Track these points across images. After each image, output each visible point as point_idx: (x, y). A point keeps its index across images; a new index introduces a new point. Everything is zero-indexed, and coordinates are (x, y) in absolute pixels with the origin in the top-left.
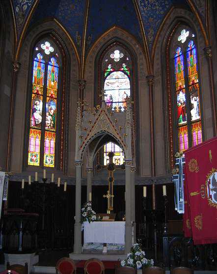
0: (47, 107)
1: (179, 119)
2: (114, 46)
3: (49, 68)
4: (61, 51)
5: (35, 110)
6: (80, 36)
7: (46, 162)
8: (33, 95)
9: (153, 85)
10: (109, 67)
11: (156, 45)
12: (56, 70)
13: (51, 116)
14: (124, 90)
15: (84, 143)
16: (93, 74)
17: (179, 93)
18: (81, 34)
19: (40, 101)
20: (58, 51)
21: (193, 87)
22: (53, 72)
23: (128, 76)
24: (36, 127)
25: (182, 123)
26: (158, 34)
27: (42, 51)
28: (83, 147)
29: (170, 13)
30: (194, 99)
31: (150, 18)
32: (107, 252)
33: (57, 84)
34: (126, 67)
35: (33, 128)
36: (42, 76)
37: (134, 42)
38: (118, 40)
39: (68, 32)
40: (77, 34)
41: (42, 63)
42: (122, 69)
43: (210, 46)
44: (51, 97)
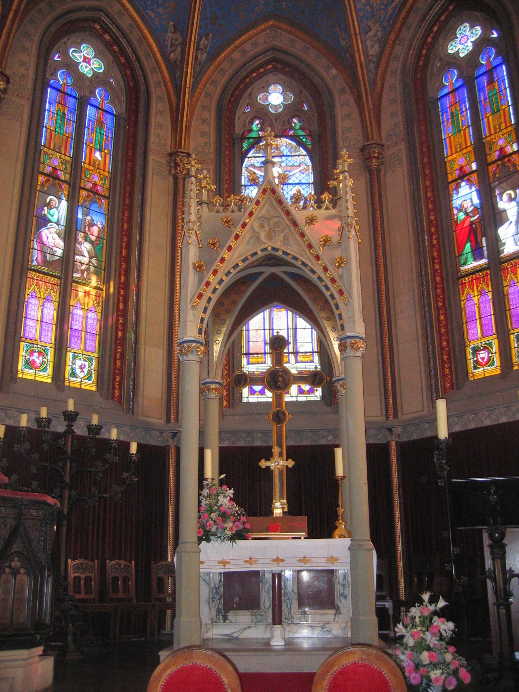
0: (80, 216)
1: (461, 254)
2: (265, 74)
3: (90, 112)
4: (124, 75)
5: (45, 221)
6: (178, 36)
7: (73, 374)
8: (41, 179)
9: (383, 168)
10: (256, 125)
12: (109, 121)
13: (91, 242)
14: (297, 187)
15: (208, 284)
16: (212, 139)
17: (458, 186)
19: (60, 199)
21: (503, 164)
23: (305, 148)
24: (45, 269)
25: (473, 264)
28: (205, 299)
30: (505, 197)
32: (286, 644)
34: (301, 128)
36: (70, 130)
37: (324, 62)
38: (279, 55)
40: (171, 28)
41: (70, 95)
42: (291, 132)
44: (94, 191)
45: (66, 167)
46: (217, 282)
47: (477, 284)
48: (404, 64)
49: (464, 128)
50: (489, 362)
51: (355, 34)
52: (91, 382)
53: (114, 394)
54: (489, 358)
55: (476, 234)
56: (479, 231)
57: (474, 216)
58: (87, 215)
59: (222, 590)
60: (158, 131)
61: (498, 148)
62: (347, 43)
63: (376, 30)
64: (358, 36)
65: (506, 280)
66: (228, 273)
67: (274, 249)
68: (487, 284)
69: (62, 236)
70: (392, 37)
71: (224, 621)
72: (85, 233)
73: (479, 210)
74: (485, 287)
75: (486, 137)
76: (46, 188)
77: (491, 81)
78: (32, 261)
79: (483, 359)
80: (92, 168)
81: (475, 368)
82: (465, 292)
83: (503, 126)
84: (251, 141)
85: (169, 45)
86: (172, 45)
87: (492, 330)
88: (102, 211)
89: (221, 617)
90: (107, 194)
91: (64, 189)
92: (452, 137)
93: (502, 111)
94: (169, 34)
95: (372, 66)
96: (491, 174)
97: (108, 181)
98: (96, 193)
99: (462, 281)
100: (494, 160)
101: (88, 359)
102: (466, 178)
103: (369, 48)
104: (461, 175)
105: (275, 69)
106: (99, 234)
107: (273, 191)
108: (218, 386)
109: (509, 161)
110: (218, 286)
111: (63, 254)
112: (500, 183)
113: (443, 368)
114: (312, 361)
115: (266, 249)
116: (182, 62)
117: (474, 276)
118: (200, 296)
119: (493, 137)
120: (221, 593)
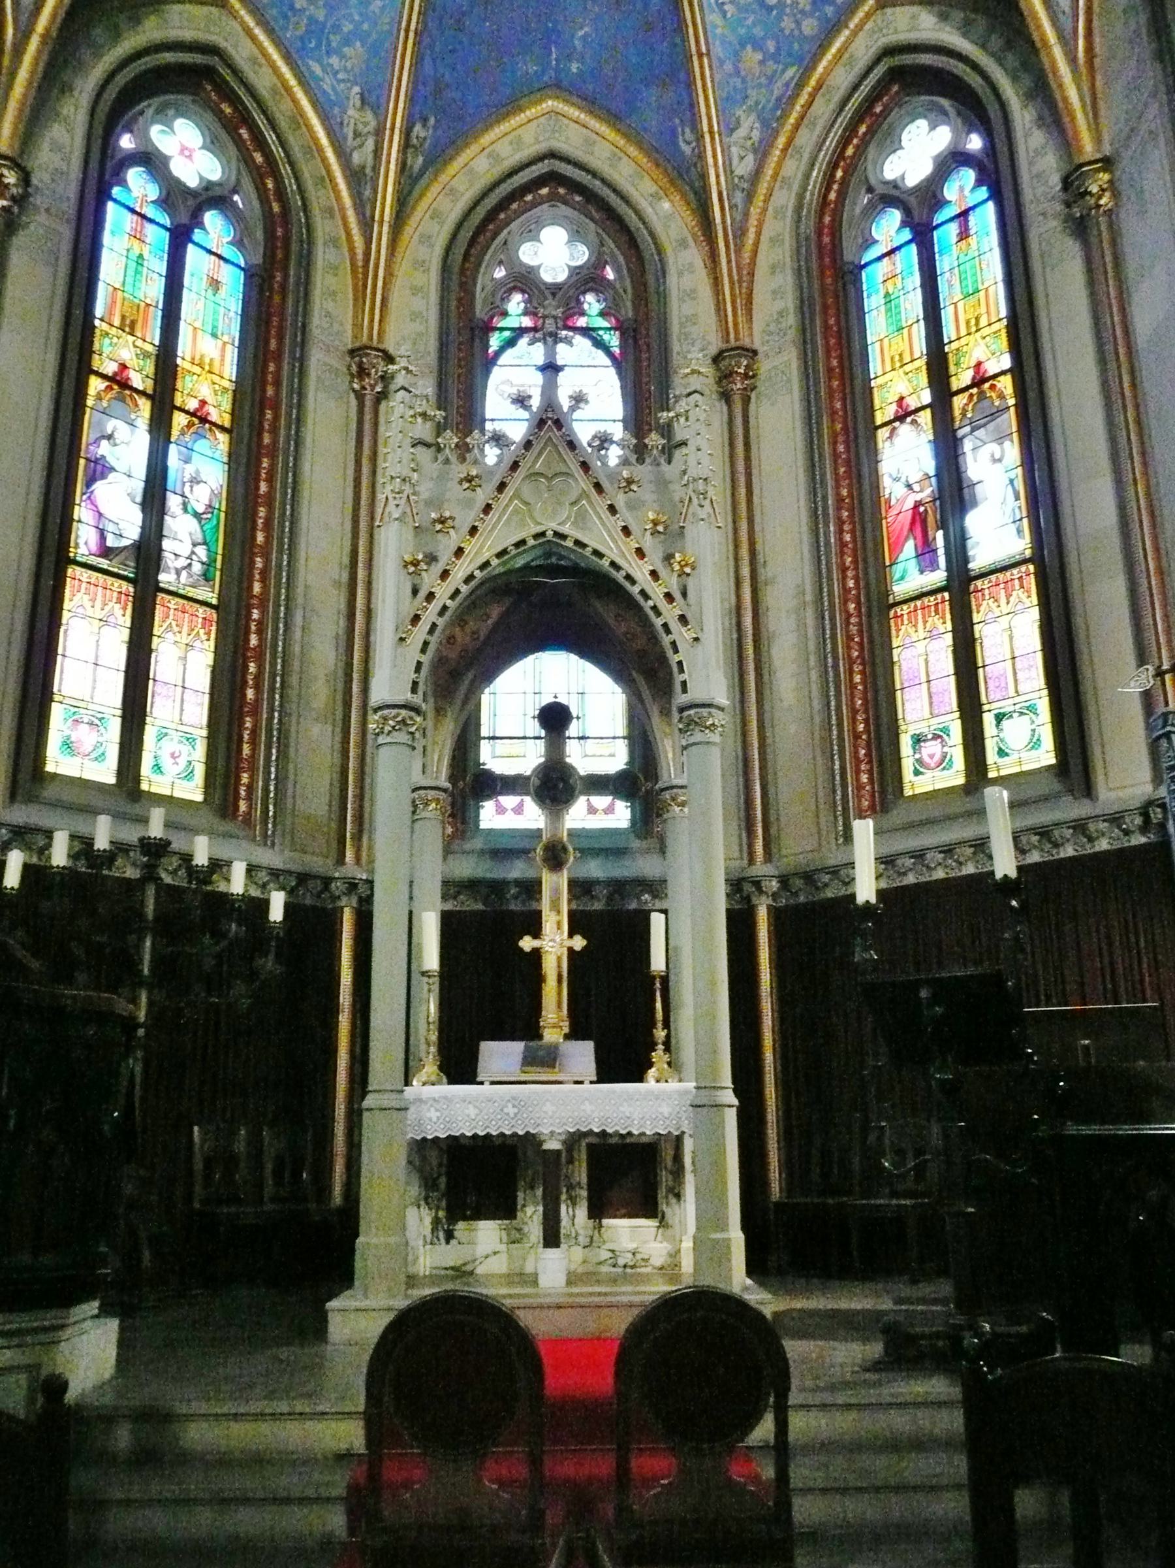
5: (99, 470)
6: (369, 116)
7: (157, 768)
8: (95, 385)
9: (753, 395)
10: (516, 303)
11: (767, 200)
12: (233, 281)
13: (197, 515)
15: (431, 596)
18: (372, 101)
20: (247, 184)
22: (215, 284)
24: (104, 563)
26: (781, 141)
27: (151, 160)
29: (855, 33)
31: (749, 48)
33: (232, 355)
34: (603, 314)
35: (85, 565)
36: (154, 290)
39: (302, 82)
43: (1107, 150)
44: (200, 417)
45: (145, 366)
46: (449, 595)
47: (924, 617)
48: (801, 197)
49: (910, 323)
50: (944, 762)
51: (711, 132)
52: (192, 784)
53: (237, 808)
54: (944, 755)
55: (924, 522)
56: (930, 519)
57: (921, 491)
58: (187, 461)
59: (443, 1181)
60: (330, 305)
61: (973, 363)
62: (693, 149)
63: (749, 127)
64: (717, 136)
65: (978, 612)
66: (469, 579)
67: (556, 534)
68: (943, 617)
69: (139, 499)
70: (781, 141)
71: (448, 1242)
72: (183, 496)
73: (933, 480)
74: (939, 623)
75: (950, 342)
76: (105, 403)
77: (964, 234)
78: (77, 546)
79: (931, 756)
80: (197, 370)
81: (917, 773)
82: (901, 633)
83: (983, 322)
84: (507, 334)
85: (351, 135)
86: (357, 134)
87: (950, 704)
88: (217, 455)
89: (441, 1235)
90: (227, 424)
91: (141, 407)
92: (886, 341)
93: (982, 293)
94: (351, 112)
95: (739, 197)
96: (957, 413)
97: (229, 397)
98: (204, 420)
99: (976, 586)
100: (964, 385)
101: (188, 739)
102: (909, 419)
103: (735, 161)
104: (901, 412)
105: (553, 198)
106: (210, 500)
107: (558, 424)
108: (442, 795)
109: (993, 387)
110: (449, 603)
111: (142, 535)
112: (973, 431)
113: (858, 772)
114: (612, 755)
115: (543, 534)
116: (376, 169)
117: (919, 603)
118: (416, 619)
119: (963, 341)
120: (443, 1186)
